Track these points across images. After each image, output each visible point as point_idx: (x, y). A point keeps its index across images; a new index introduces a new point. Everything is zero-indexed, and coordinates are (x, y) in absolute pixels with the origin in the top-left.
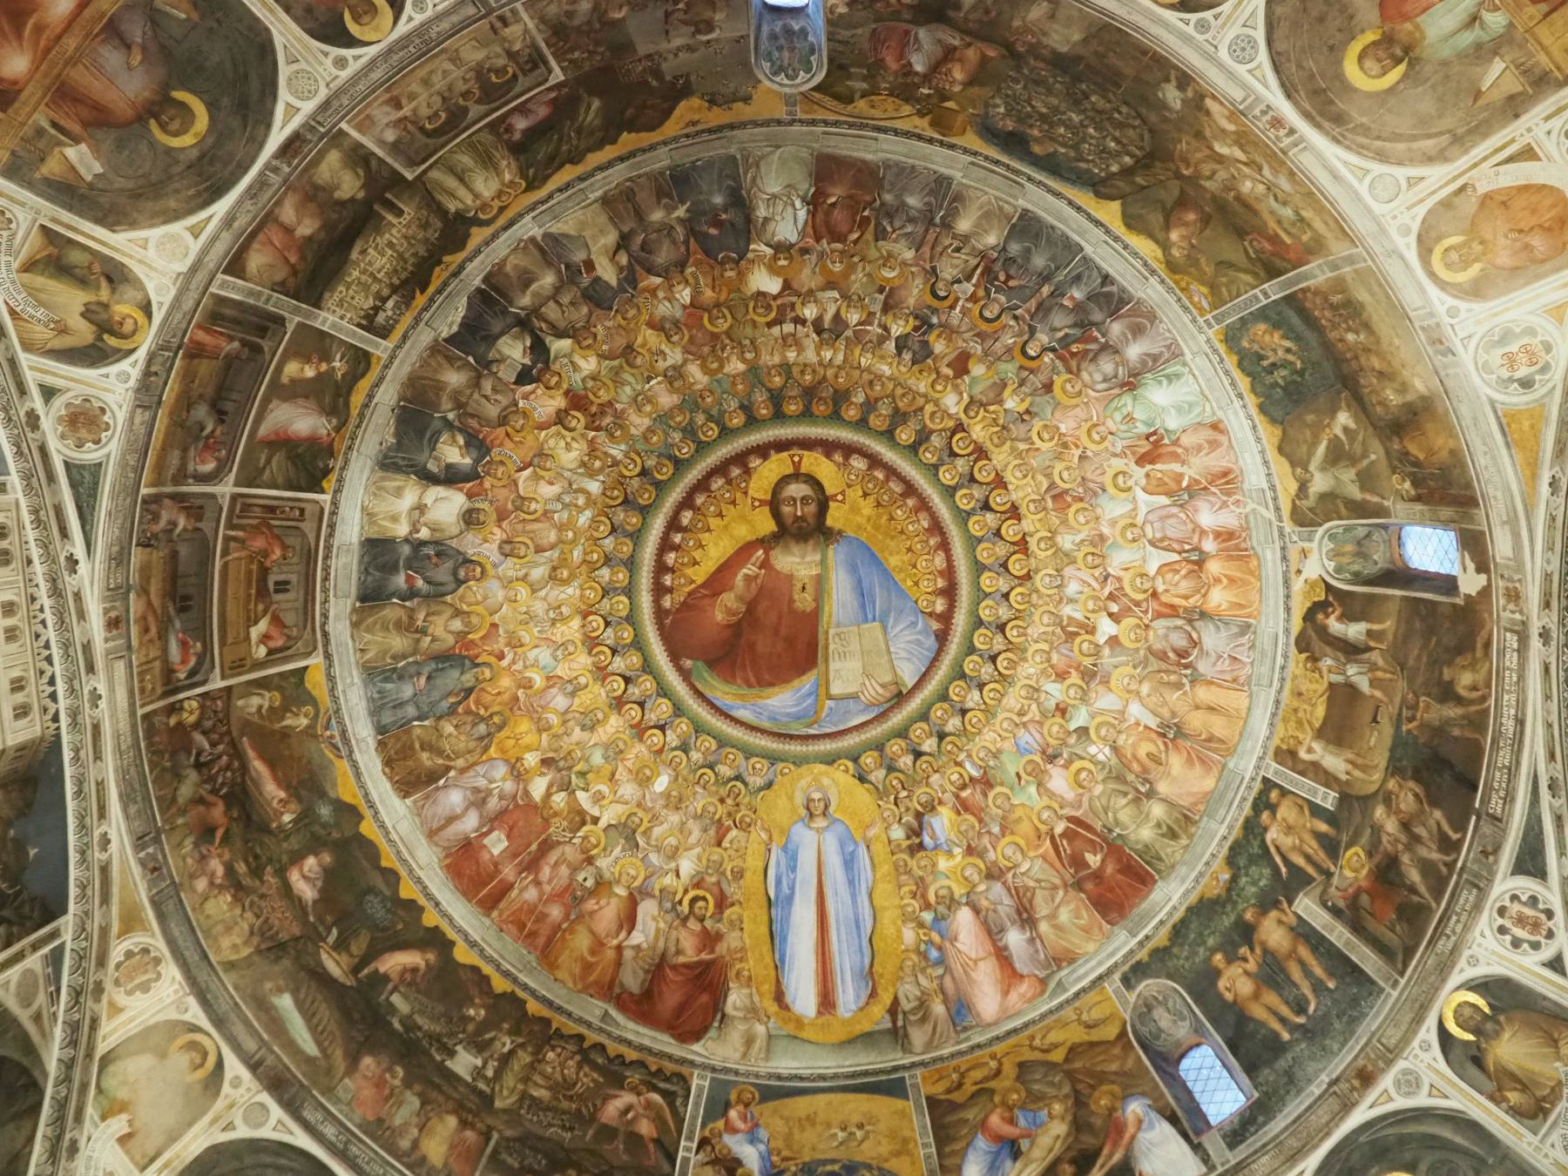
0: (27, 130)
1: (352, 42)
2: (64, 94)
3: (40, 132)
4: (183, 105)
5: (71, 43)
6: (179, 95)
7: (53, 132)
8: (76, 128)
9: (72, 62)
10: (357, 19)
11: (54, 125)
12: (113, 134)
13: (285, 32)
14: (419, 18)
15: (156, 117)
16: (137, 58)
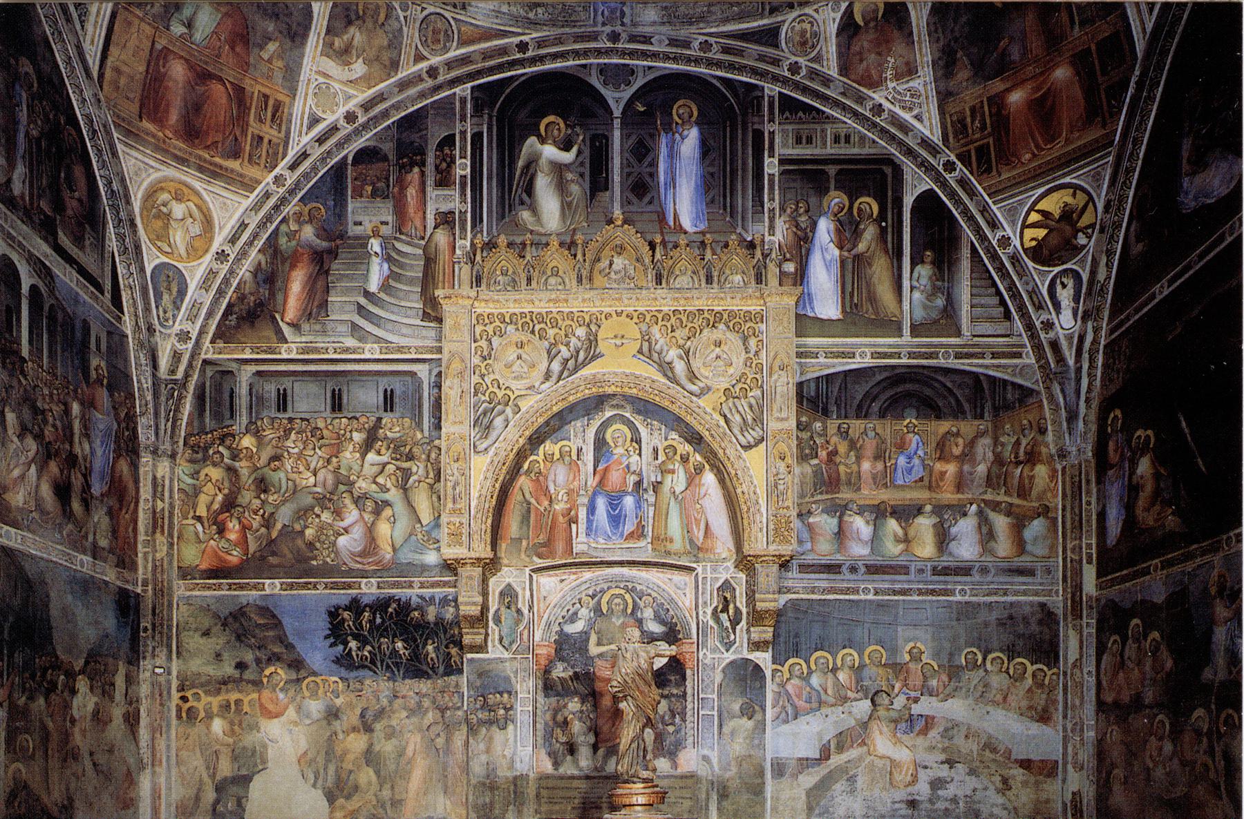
3: (1082, 24)
7: (1076, 18)
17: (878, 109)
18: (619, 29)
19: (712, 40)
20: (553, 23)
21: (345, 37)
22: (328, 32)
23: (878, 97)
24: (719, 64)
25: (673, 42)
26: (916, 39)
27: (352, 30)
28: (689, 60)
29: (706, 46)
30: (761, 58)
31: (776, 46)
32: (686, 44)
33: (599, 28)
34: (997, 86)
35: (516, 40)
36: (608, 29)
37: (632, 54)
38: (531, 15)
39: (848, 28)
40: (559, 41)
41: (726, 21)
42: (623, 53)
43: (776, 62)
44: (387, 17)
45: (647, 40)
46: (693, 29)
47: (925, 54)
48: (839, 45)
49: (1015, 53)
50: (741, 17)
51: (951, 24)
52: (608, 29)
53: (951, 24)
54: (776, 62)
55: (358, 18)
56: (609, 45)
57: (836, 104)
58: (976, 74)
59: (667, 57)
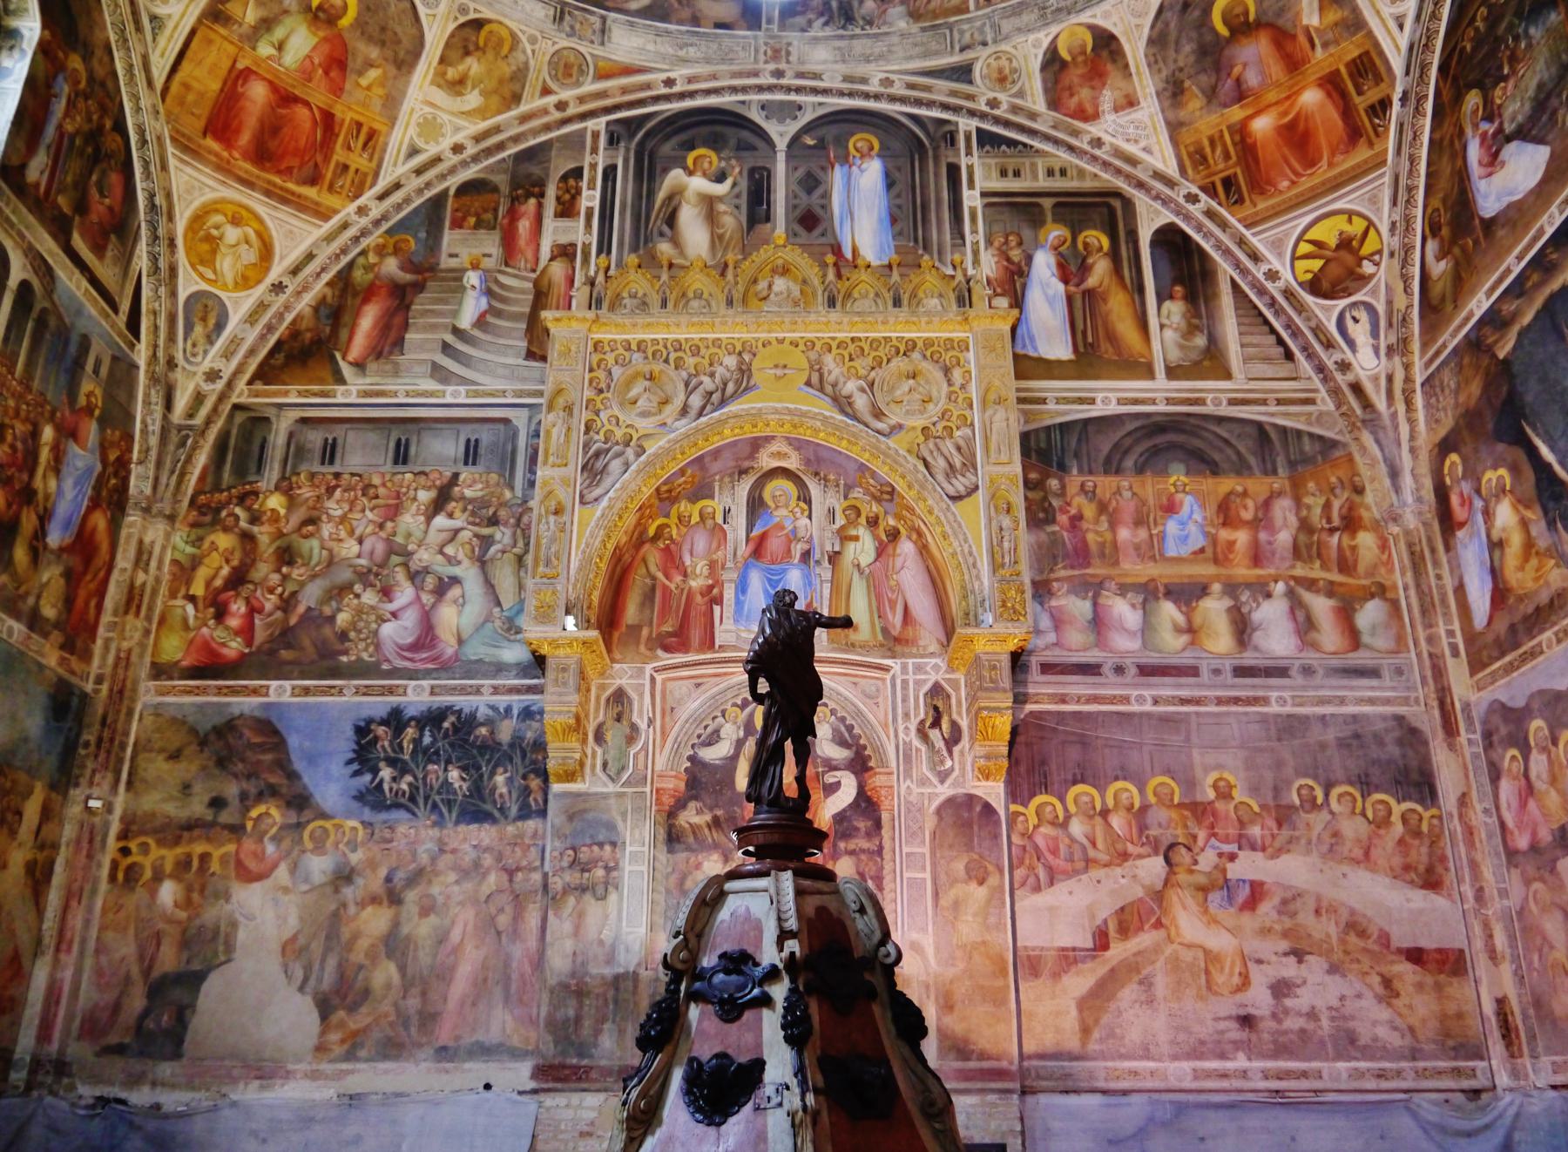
0: (1332, 50)
1: (1093, 28)
2: (1294, 64)
3: (1325, 45)
4: (1225, 22)
5: (1272, 96)
6: (1223, 31)
8: (1302, 39)
9: (1278, 85)
10: (1084, 46)
11: (1313, 46)
12: (1280, 22)
13: (1135, 49)
14: (1041, 35)
15: (1247, 22)
16: (1236, 70)
17: (1098, 142)
18: (783, 66)
19: (893, 77)
20: (708, 61)
21: (461, 68)
22: (442, 60)
23: (1094, 129)
24: (902, 100)
25: (847, 79)
26: (1133, 69)
27: (469, 60)
28: (867, 96)
29: (887, 82)
30: (954, 93)
31: (970, 82)
32: (864, 81)
33: (761, 66)
34: (1236, 113)
35: (664, 76)
36: (772, 66)
37: (798, 90)
38: (682, 53)
39: (1053, 63)
40: (714, 77)
41: (910, 58)
42: (789, 89)
43: (971, 97)
44: (512, 49)
45: (817, 76)
46: (872, 66)
47: (1146, 84)
48: (1044, 81)
49: (1252, 79)
50: (926, 55)
51: (1171, 53)
52: (772, 66)
53: (1171, 53)
54: (971, 97)
55: (478, 48)
56: (773, 81)
57: (1047, 138)
58: (1209, 102)
59: (841, 94)
